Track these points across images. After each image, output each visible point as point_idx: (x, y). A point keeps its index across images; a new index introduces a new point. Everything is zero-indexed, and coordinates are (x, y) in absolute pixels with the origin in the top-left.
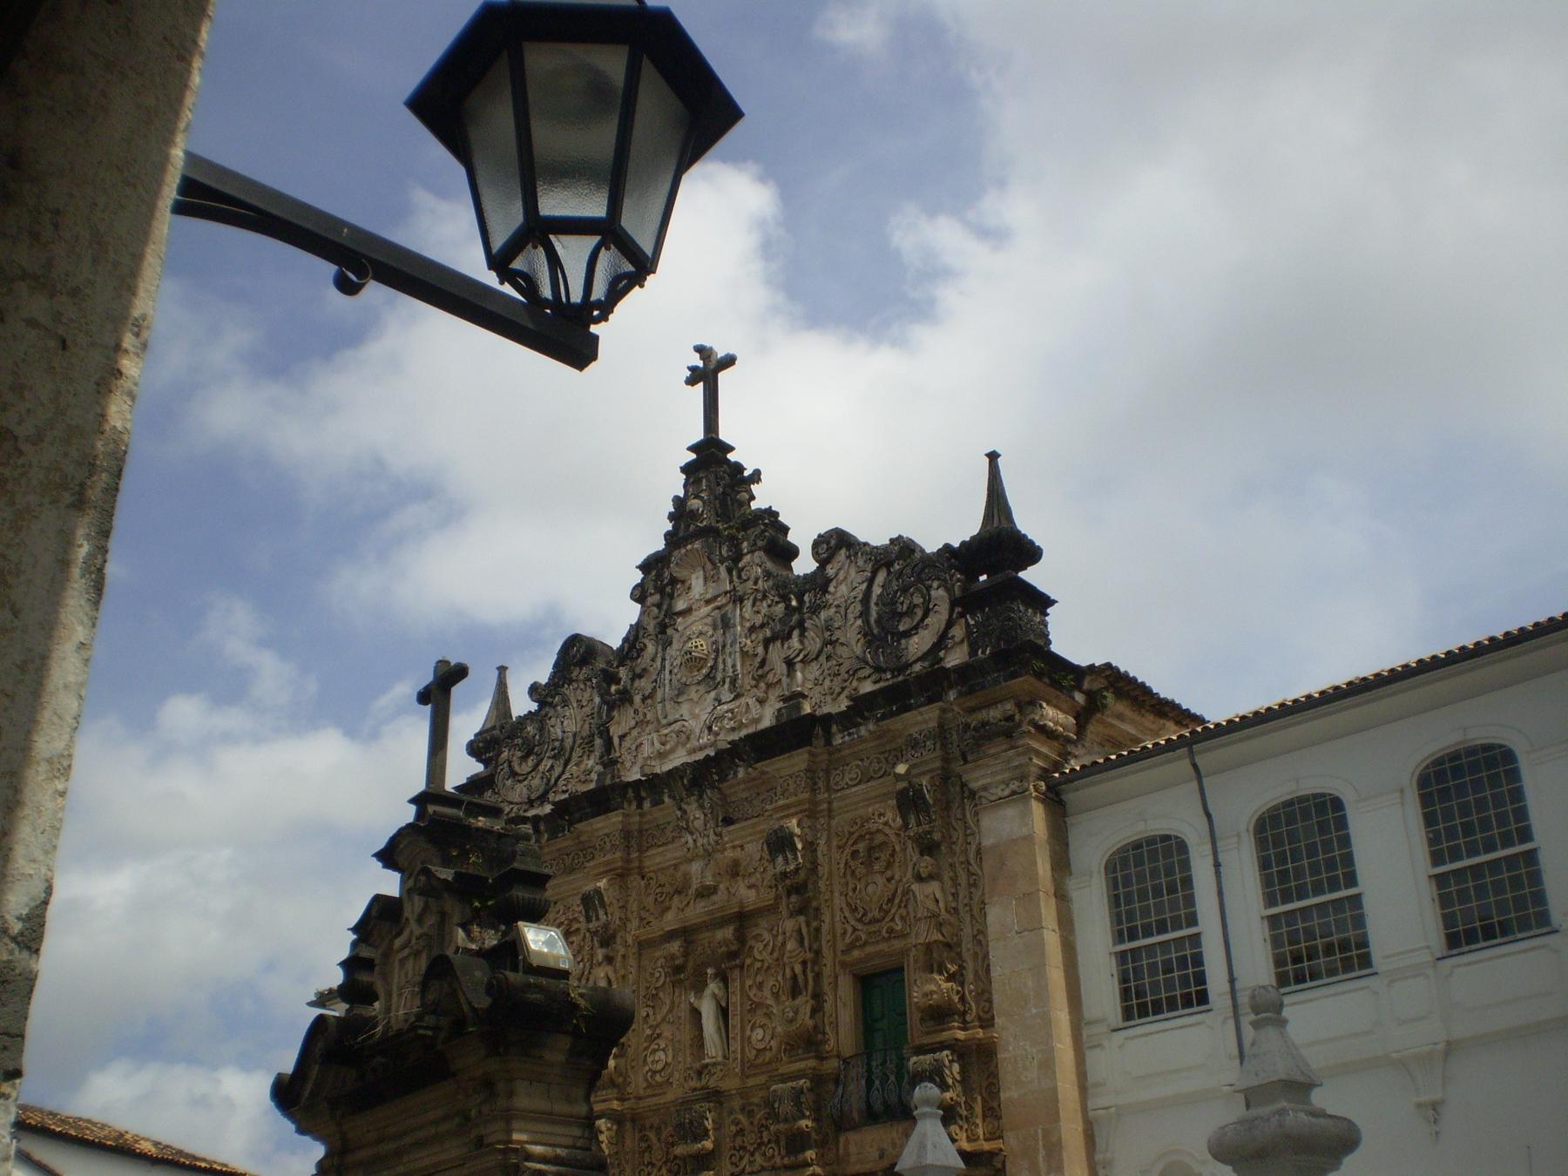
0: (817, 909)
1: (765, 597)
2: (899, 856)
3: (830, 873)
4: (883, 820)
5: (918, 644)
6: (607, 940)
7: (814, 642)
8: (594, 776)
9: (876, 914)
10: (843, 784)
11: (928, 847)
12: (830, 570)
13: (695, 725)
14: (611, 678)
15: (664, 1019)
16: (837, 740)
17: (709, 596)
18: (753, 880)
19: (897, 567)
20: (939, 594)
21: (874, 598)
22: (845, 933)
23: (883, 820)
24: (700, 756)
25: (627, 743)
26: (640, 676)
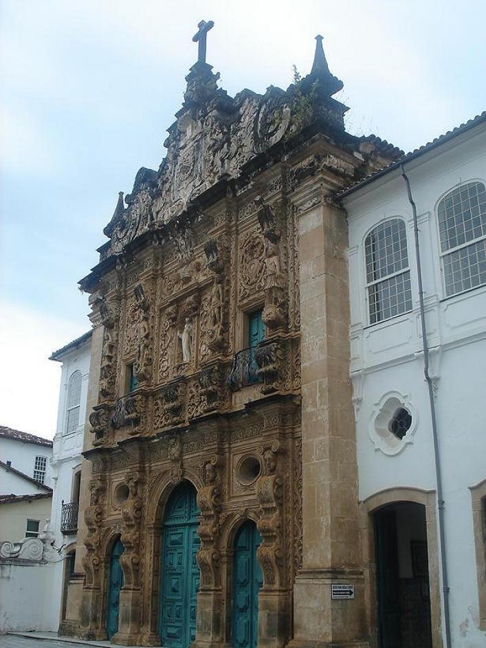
0: (228, 280)
3: (236, 262)
6: (146, 309)
7: (234, 147)
9: (254, 279)
11: (274, 238)
15: (168, 346)
16: (239, 194)
18: (205, 272)
22: (240, 292)
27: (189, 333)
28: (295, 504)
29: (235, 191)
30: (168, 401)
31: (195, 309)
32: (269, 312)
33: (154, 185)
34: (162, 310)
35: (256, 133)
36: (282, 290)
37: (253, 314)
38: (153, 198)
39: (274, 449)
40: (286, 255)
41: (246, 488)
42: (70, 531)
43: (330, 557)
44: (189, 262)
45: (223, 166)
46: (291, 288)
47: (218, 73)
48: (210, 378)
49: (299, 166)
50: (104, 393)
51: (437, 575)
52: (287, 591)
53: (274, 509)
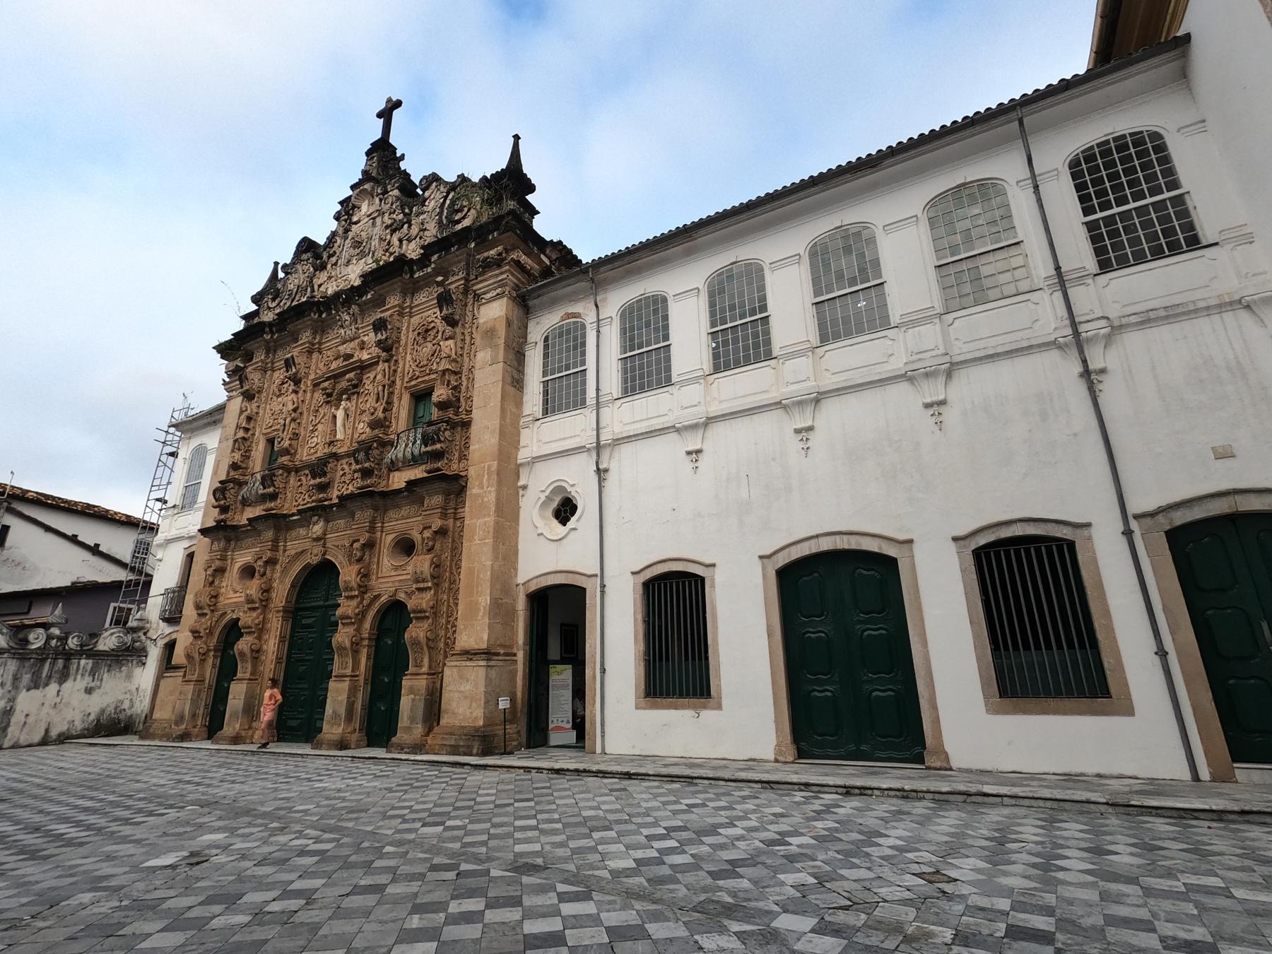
6: (297, 381)
12: (427, 194)
16: (416, 275)
27: (346, 410)
28: (451, 583)
30: (314, 478)
31: (355, 386)
32: (440, 393)
33: (318, 256)
34: (316, 385)
36: (455, 373)
37: (421, 397)
38: (316, 270)
39: (434, 528)
40: (463, 340)
41: (396, 568)
42: (172, 618)
43: (486, 637)
44: (352, 340)
45: (400, 247)
46: (465, 372)
47: (403, 155)
48: (367, 454)
49: (486, 254)
50: (234, 466)
51: (594, 656)
52: (436, 674)
53: (430, 588)
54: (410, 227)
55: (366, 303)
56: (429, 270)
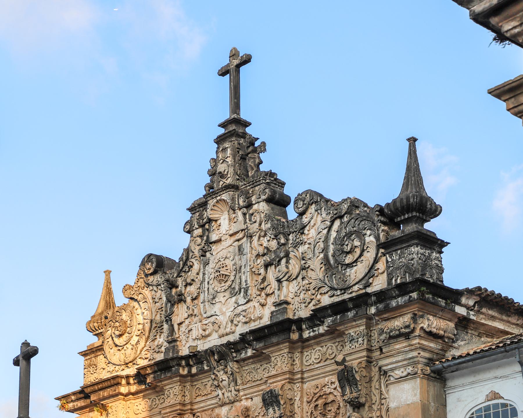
1: (265, 235)
2: (342, 410)
4: (334, 386)
5: (357, 272)
7: (294, 267)
8: (163, 349)
10: (310, 362)
12: (305, 219)
13: (223, 319)
14: (172, 285)
17: (231, 232)
19: (345, 219)
20: (370, 239)
21: (332, 240)
23: (334, 386)
24: (224, 340)
25: (183, 328)
26: (191, 284)
29: (300, 330)
35: (326, 258)
47: (264, 144)
54: (287, 262)
55: (244, 360)
56: (322, 330)
